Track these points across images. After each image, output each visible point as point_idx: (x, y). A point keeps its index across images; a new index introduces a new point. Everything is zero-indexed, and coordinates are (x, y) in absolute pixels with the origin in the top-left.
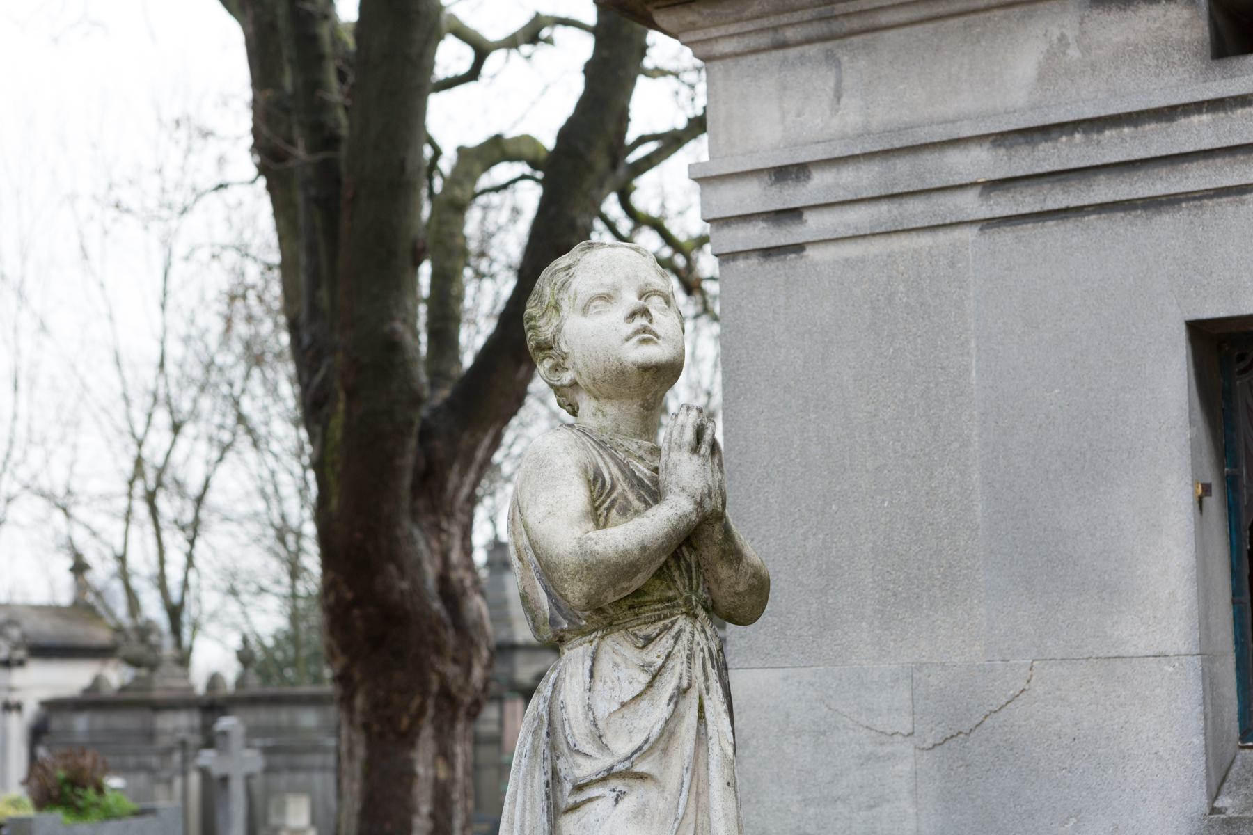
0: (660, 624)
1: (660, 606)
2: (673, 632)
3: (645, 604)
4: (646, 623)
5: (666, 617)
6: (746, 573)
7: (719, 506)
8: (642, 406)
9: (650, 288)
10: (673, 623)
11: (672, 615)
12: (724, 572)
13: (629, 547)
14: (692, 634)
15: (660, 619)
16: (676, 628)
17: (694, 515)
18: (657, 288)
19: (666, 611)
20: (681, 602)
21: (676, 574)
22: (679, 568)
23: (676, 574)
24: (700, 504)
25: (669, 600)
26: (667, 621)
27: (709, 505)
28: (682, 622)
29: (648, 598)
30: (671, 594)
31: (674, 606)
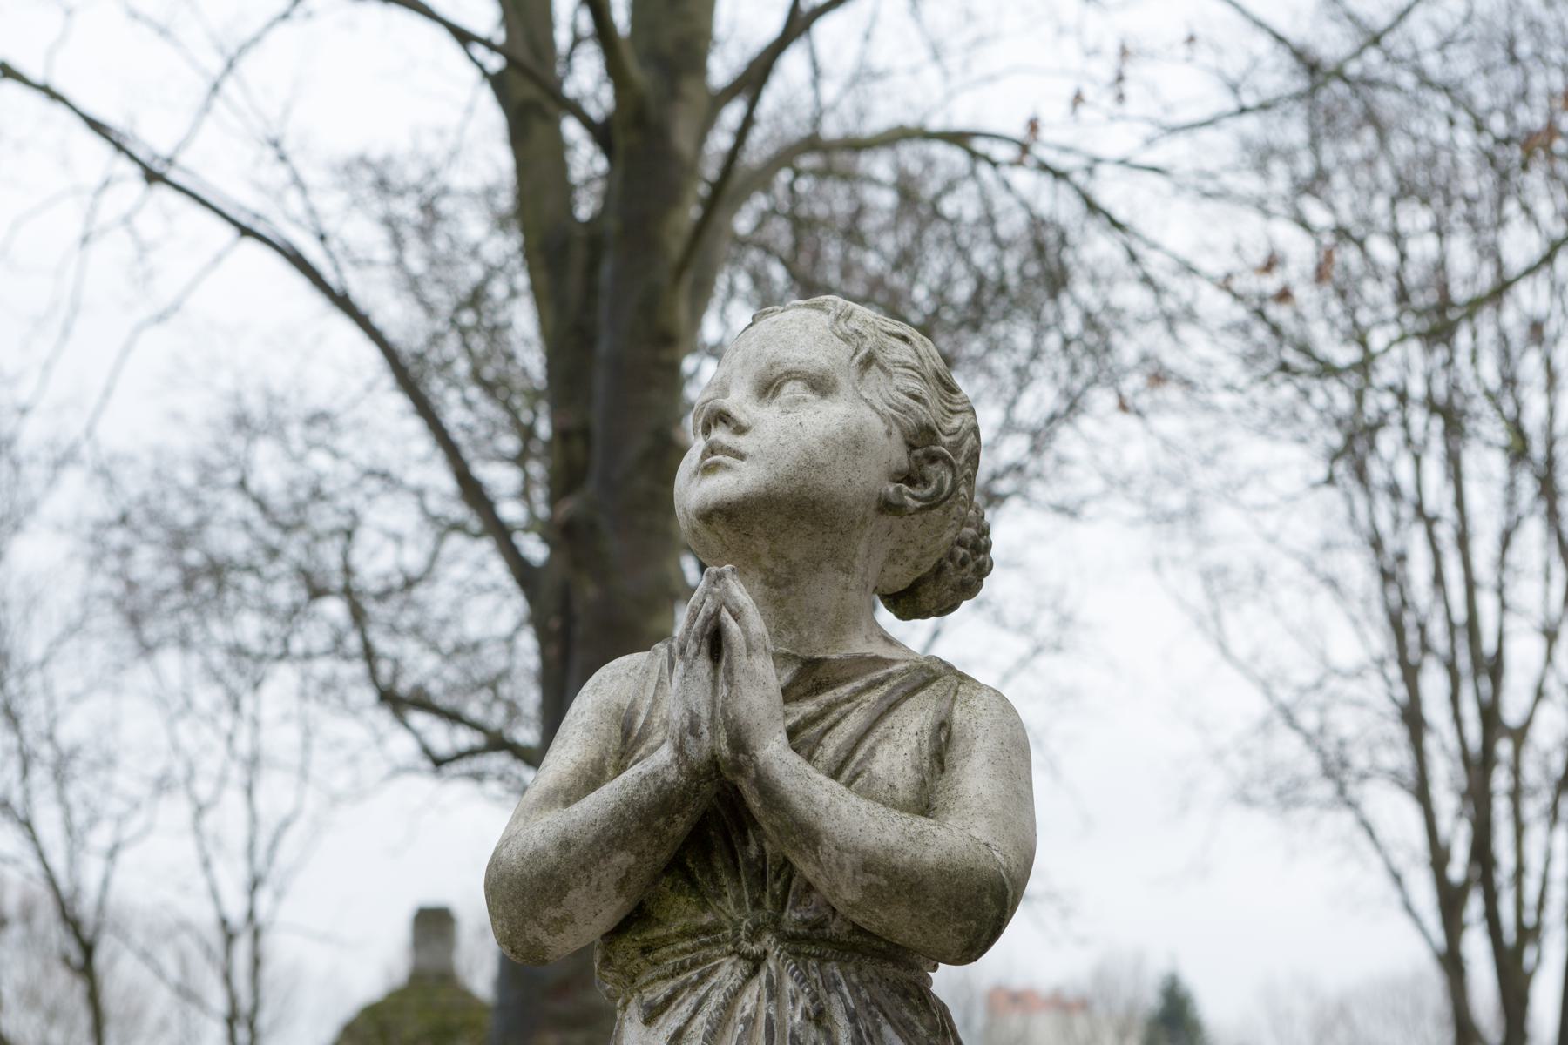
0: (682, 978)
1: (688, 944)
2: (702, 991)
3: (665, 941)
4: (659, 978)
5: (694, 964)
6: (841, 867)
7: (725, 751)
8: (766, 582)
9: (779, 371)
10: (703, 978)
11: (707, 960)
12: (807, 869)
13: (541, 844)
14: (736, 993)
15: (683, 968)
16: (714, 980)
17: (674, 770)
18: (790, 366)
19: (705, 951)
20: (729, 932)
21: (725, 880)
22: (735, 871)
23: (725, 880)
24: (680, 749)
25: (706, 931)
26: (693, 975)
27: (698, 751)
28: (728, 972)
29: (659, 932)
30: (706, 919)
31: (717, 942)
